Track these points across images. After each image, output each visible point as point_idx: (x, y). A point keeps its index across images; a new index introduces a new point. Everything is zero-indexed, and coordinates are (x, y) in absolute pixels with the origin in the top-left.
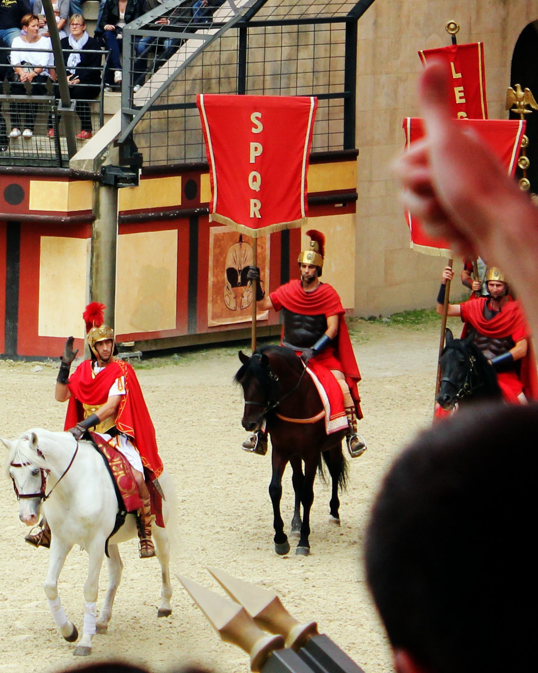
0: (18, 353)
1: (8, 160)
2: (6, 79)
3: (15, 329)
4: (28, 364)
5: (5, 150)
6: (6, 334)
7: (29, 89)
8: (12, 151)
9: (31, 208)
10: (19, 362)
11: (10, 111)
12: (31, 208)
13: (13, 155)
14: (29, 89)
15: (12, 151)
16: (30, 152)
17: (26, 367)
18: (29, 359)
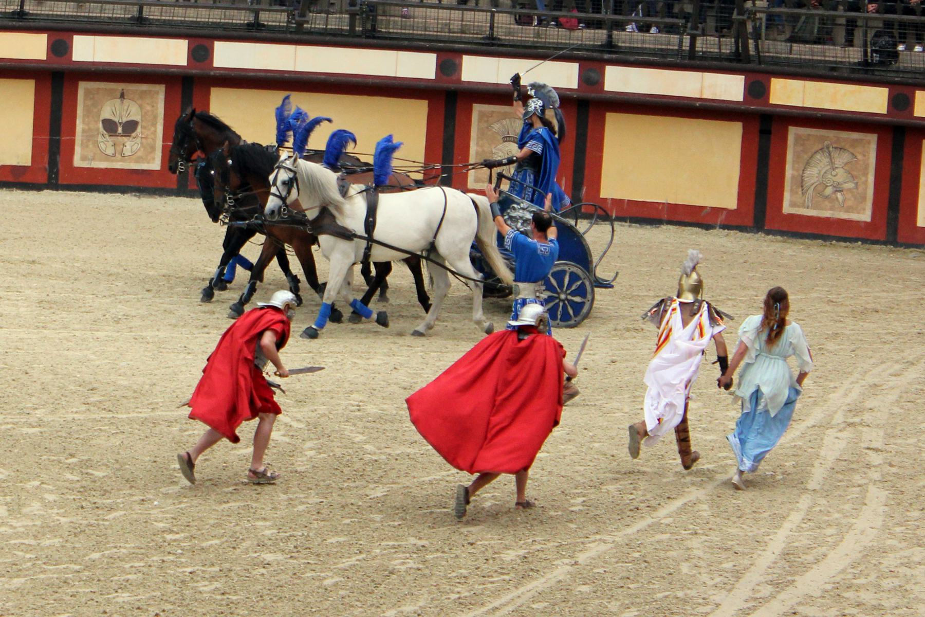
0: (898, 240)
1: (897, 71)
2: (899, 2)
3: (896, 219)
4: (906, 250)
5: (896, 63)
6: (888, 223)
7: (918, 11)
8: (901, 64)
9: (916, 115)
10: (898, 249)
11: (900, 29)
12: (916, 115)
13: (902, 68)
14: (918, 11)
15: (901, 64)
16: (918, 66)
17: (905, 252)
18: (908, 246)
